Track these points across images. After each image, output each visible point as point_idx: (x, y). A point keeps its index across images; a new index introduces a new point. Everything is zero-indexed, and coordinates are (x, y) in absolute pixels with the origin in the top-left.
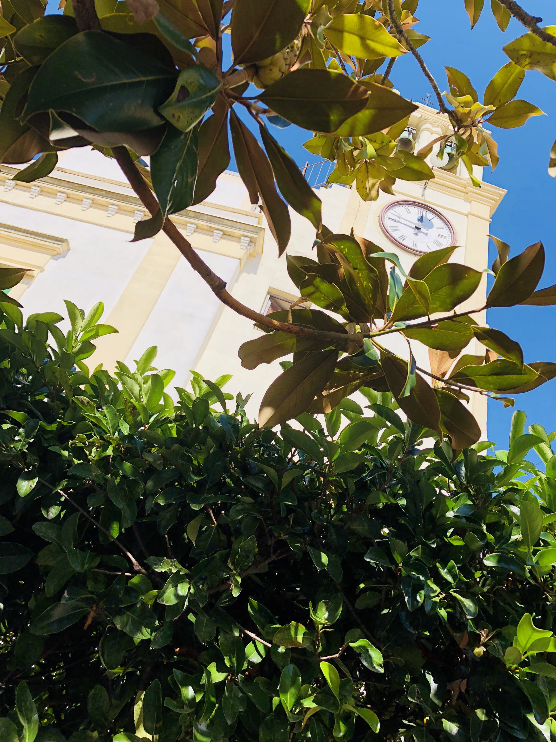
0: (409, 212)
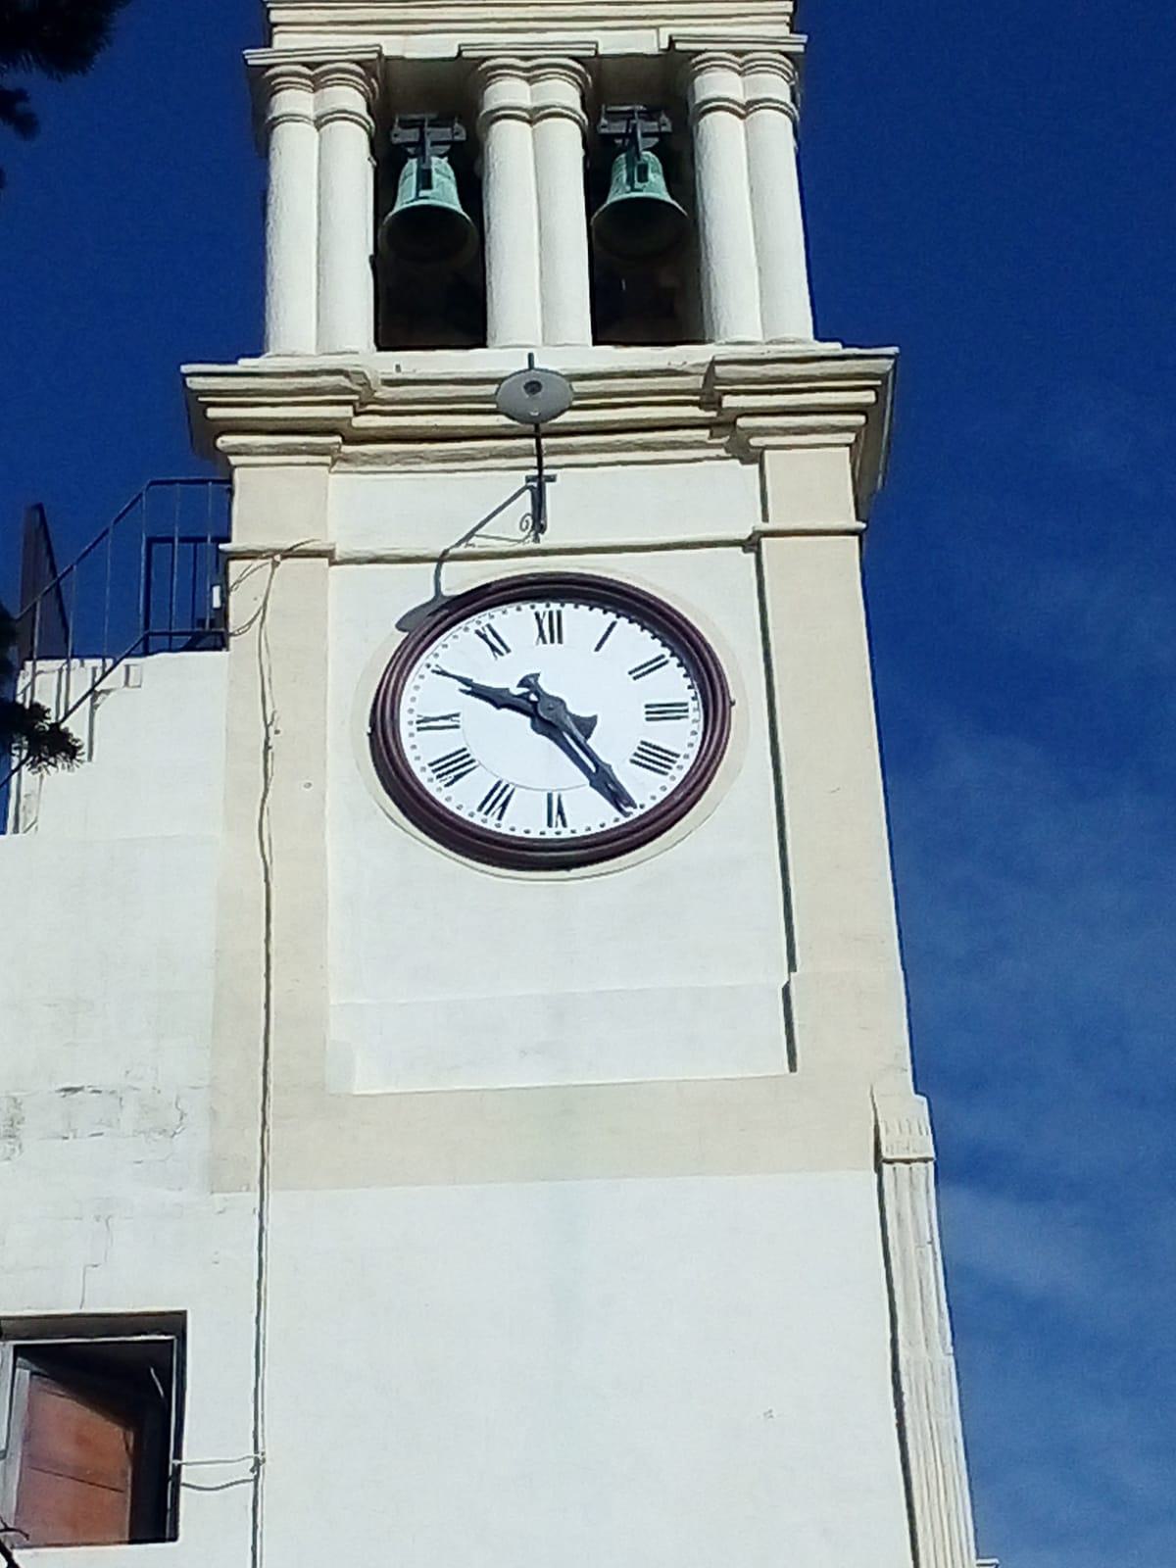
0: (497, 646)
